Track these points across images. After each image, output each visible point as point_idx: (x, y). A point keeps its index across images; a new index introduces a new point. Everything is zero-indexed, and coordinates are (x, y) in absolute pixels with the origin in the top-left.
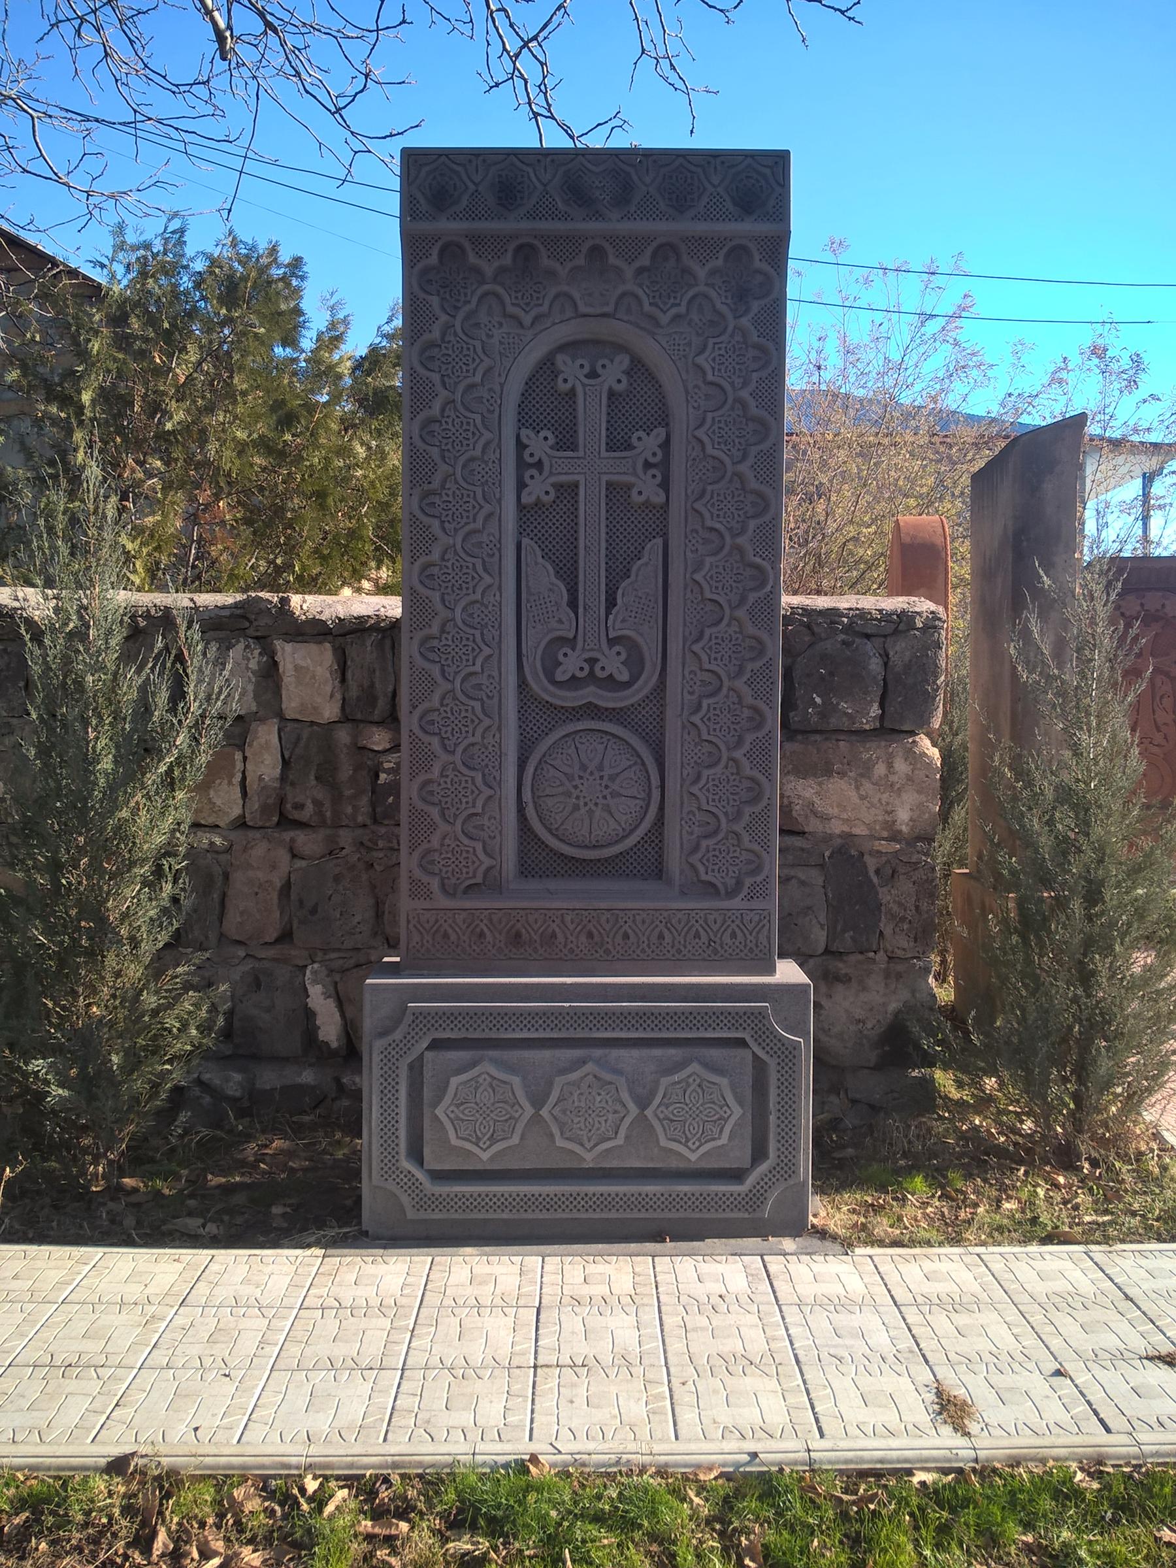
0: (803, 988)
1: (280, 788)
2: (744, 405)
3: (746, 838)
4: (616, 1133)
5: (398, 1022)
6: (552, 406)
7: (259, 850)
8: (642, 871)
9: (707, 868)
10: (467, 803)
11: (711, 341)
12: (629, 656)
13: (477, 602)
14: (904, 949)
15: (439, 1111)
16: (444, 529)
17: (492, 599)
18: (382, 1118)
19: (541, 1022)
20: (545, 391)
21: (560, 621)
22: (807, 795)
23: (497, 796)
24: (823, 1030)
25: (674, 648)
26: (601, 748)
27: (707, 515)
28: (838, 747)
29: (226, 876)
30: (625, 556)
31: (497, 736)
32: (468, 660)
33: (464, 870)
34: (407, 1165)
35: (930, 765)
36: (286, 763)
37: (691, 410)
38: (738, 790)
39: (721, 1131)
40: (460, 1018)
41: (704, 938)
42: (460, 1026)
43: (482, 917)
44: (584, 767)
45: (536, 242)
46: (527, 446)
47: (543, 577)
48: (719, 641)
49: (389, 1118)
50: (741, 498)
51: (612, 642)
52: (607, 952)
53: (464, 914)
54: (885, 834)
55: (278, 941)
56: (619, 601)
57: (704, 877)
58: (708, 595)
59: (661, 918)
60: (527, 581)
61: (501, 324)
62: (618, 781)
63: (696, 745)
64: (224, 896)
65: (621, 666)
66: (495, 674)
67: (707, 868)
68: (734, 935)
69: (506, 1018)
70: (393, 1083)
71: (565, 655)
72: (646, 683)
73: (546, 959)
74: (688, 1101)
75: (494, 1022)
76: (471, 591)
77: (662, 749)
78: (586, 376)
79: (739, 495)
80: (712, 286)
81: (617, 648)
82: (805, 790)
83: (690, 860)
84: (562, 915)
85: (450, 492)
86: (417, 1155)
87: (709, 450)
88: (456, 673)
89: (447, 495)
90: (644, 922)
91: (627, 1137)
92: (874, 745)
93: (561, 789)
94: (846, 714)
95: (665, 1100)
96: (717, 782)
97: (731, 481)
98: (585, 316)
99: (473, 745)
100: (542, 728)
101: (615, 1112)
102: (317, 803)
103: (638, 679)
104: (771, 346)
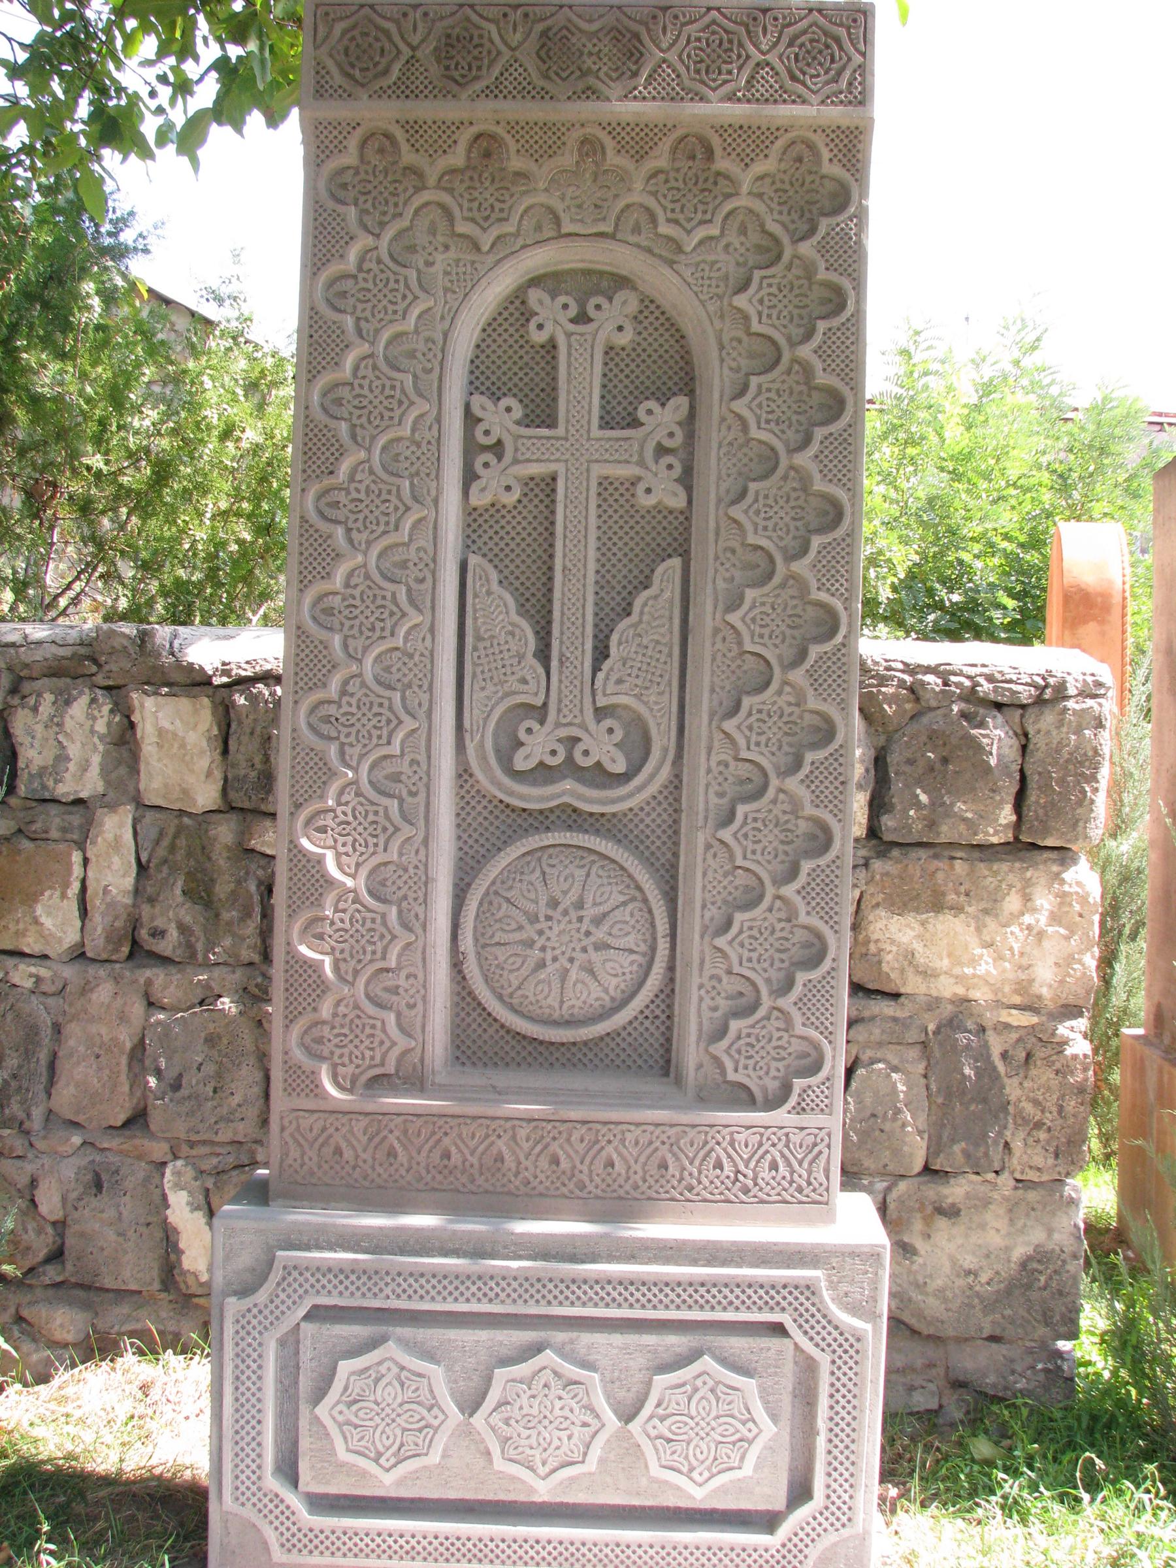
0: (874, 1256)
1: (134, 906)
2: (807, 371)
3: (798, 1019)
4: (585, 1454)
5: (264, 1278)
6: (520, 363)
7: (103, 993)
8: (640, 1062)
9: (737, 1062)
10: (374, 953)
11: (757, 274)
12: (626, 735)
13: (397, 649)
14: (1039, 1169)
15: (322, 1410)
16: (351, 541)
17: (420, 647)
18: (238, 1416)
19: (474, 1289)
20: (511, 341)
21: (524, 681)
22: (905, 940)
23: (420, 943)
24: (917, 1286)
25: (700, 723)
26: (580, 874)
27: (749, 527)
28: (952, 867)
29: (57, 1029)
30: (625, 582)
31: (422, 852)
32: (380, 737)
33: (368, 1053)
34: (272, 1483)
35: (1084, 899)
36: (142, 868)
37: (726, 371)
38: (787, 945)
39: (742, 1458)
40: (353, 1277)
41: (728, 1169)
42: (352, 1288)
43: (392, 1125)
44: (554, 903)
45: (500, 131)
46: (480, 420)
47: (499, 612)
48: (764, 716)
49: (248, 1417)
50: (801, 502)
51: (601, 713)
52: (582, 1186)
53: (364, 1122)
54: (1017, 1000)
55: (127, 1124)
56: (613, 650)
57: (731, 1076)
58: (748, 647)
59: (664, 1137)
60: (475, 619)
61: (447, 248)
62: (605, 927)
63: (725, 875)
64: (54, 1056)
65: (612, 748)
66: (422, 758)
67: (737, 1062)
68: (774, 1166)
69: (423, 1281)
70: (254, 1366)
71: (529, 731)
72: (652, 776)
73: (486, 1192)
74: (693, 1413)
75: (405, 1285)
76: (387, 633)
77: (675, 877)
78: (571, 321)
79: (797, 499)
80: (760, 196)
81: (608, 723)
82: (896, 932)
83: (711, 1049)
84: (514, 1127)
85: (362, 487)
86: (289, 1471)
87: (754, 433)
88: (362, 756)
89: (358, 491)
90: (637, 1143)
91: (602, 1461)
92: (1005, 866)
93: (517, 936)
94: (965, 820)
95: (660, 1411)
96: (755, 933)
97: (785, 478)
98: (569, 235)
99: (386, 864)
100: (493, 840)
101: (585, 1425)
102: (183, 928)
103: (638, 770)
104: (846, 284)
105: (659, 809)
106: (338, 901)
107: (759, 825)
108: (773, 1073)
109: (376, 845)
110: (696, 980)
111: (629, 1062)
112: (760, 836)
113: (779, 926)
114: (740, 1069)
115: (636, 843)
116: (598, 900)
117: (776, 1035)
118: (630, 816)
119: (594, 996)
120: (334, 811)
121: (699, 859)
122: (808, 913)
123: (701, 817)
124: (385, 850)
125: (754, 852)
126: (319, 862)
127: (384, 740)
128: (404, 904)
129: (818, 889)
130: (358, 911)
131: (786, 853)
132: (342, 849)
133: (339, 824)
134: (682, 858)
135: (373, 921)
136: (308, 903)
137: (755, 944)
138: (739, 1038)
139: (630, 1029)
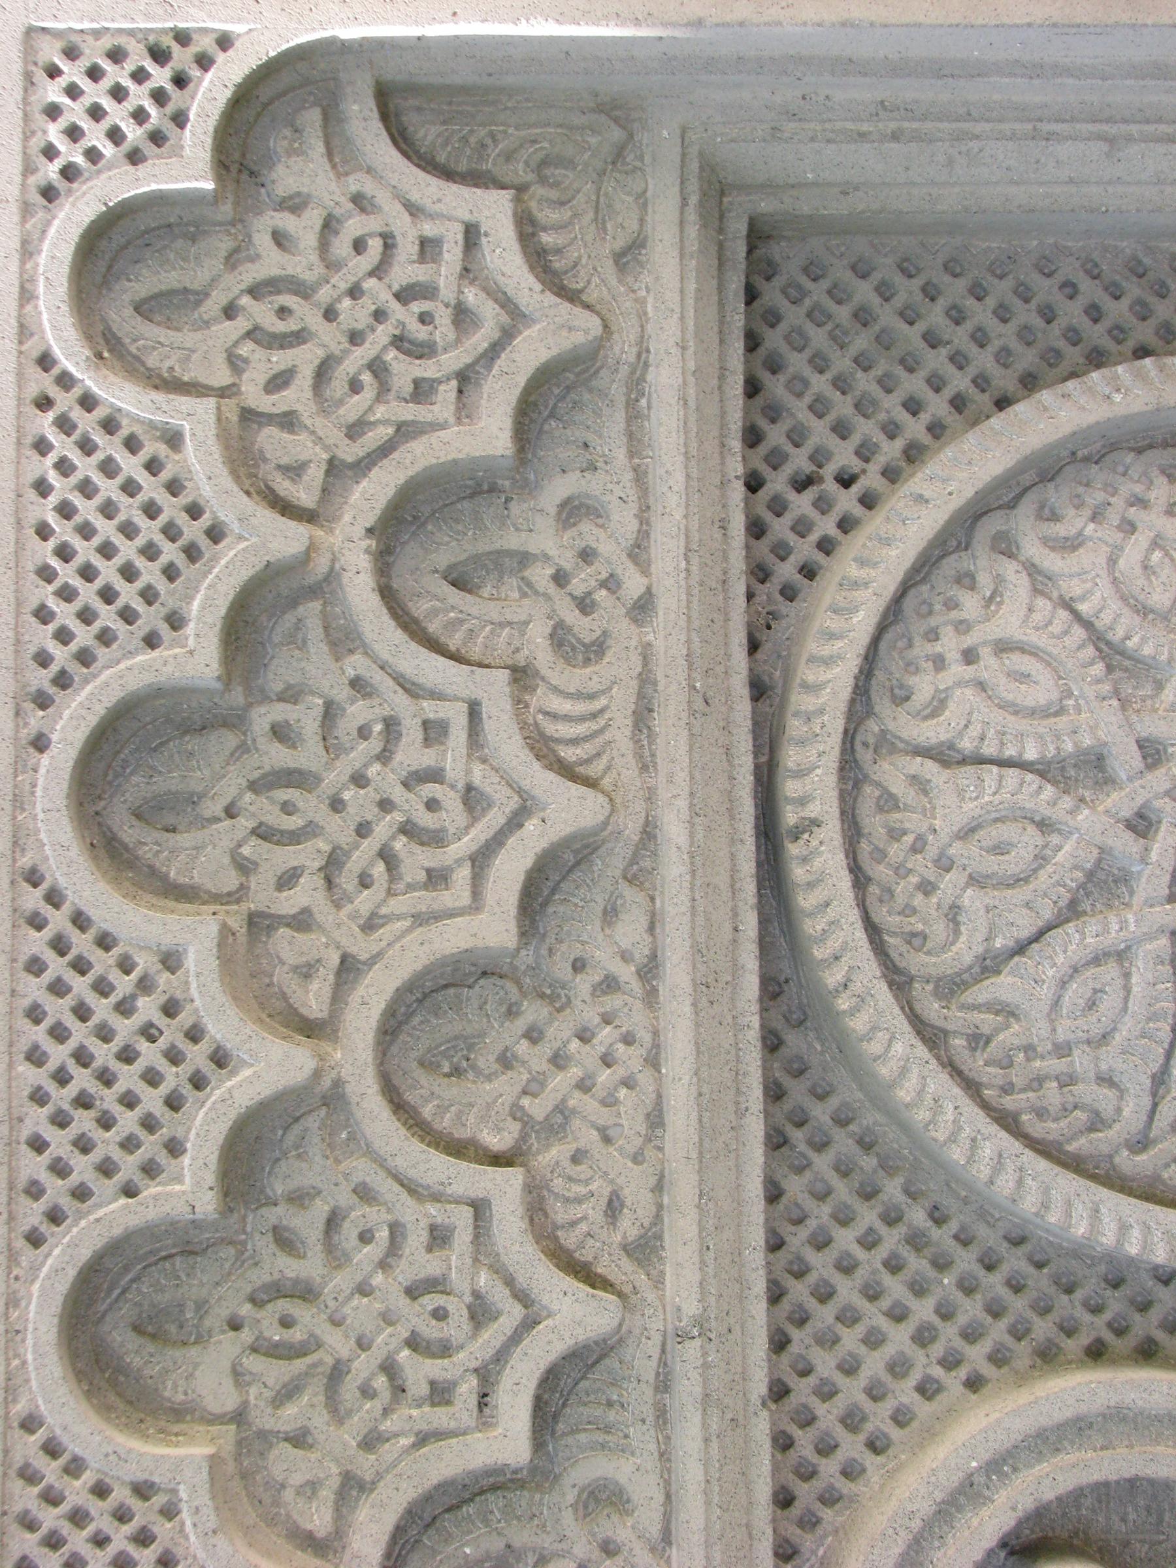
3: (202, 464)
8: (864, 292)
57: (494, 210)
63: (558, 1122)
96: (416, 860)
105: (852, 1391)
107: (419, 1372)
108: (304, 228)
110: (668, 636)
111: (907, 290)
112: (416, 1316)
113: (306, 893)
114: (453, 238)
115: (943, 1237)
116: (1110, 972)
117: (297, 397)
118: (976, 1355)
119: (1091, 558)
121: (684, 1186)
122: (170, 961)
123: (688, 1387)
125: (439, 1237)
129: (128, 1078)
131: (285, 1241)
134: (755, 1188)
137: (411, 805)
138: (465, 379)
139: (915, 428)
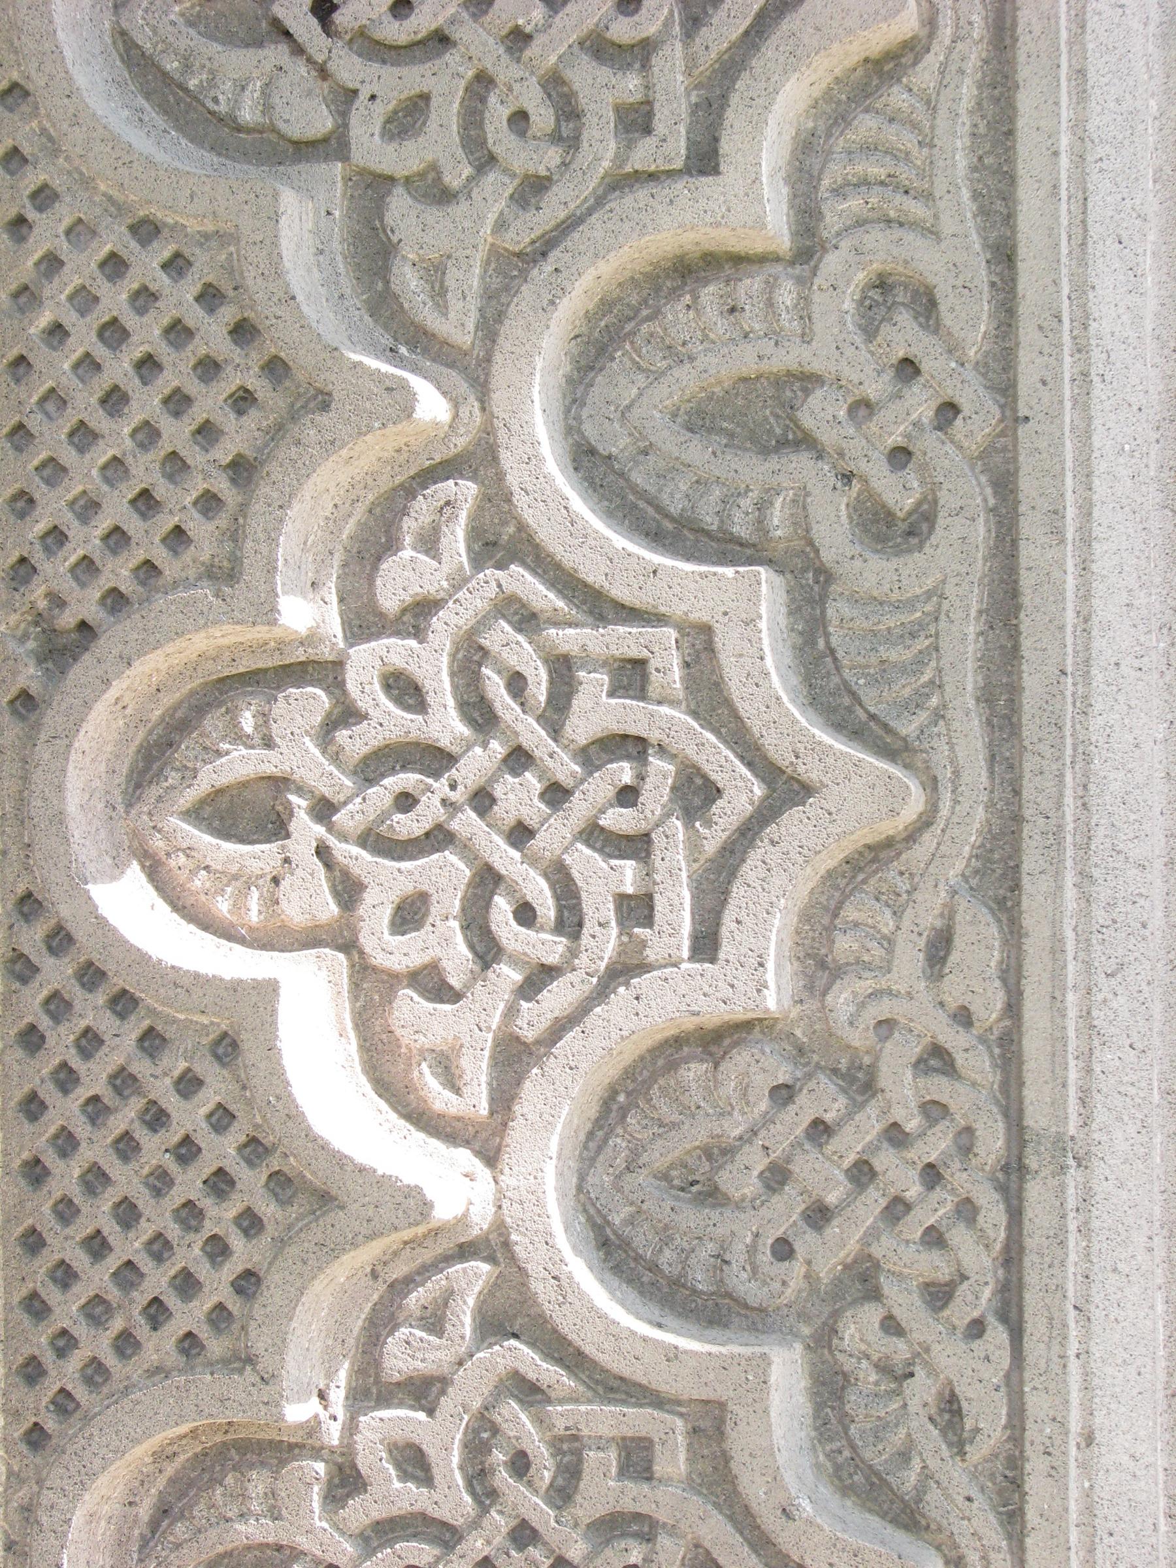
31: (975, 975)
32: (636, 120)
66: (951, 260)
88: (514, 267)
99: (716, 1041)
106: (381, 1323)
109: (637, 909)
120: (329, 673)
124: (706, 945)
126: (226, 1048)
127: (671, 140)
128: (860, 1329)
130: (528, 1391)
132: (395, 952)
133: (371, 768)
135: (637, 1459)
136: (159, 1346)
